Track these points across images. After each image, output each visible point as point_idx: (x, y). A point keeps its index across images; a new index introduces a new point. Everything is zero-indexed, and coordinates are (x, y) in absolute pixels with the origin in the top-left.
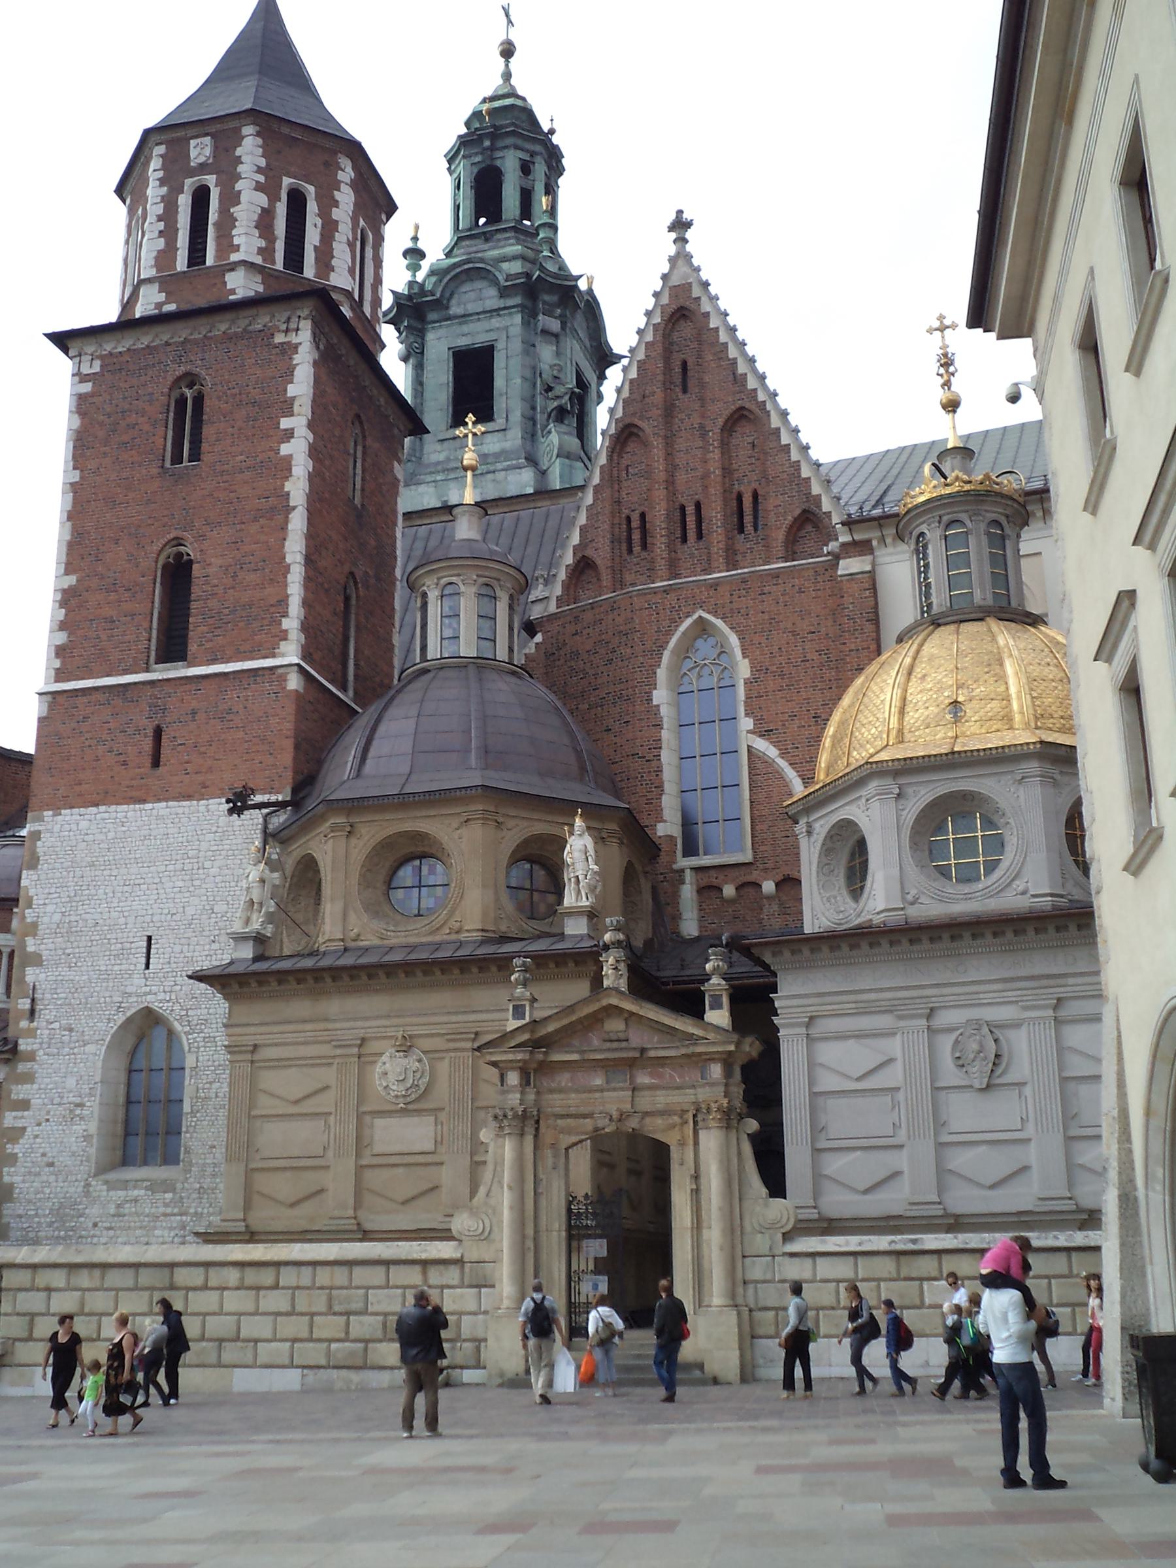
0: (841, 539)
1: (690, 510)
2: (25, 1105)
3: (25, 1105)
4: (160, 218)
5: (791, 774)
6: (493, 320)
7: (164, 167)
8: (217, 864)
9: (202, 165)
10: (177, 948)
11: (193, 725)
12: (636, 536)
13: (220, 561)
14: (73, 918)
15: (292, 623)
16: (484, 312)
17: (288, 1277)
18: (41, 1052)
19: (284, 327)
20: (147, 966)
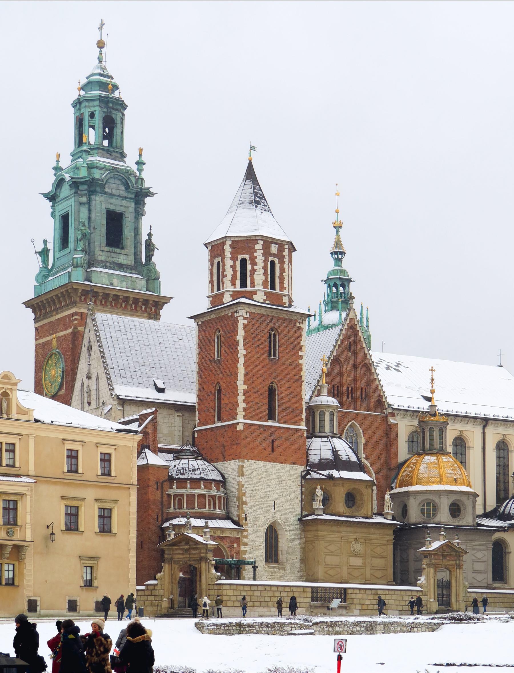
0: (390, 411)
1: (350, 389)
2: (246, 544)
3: (246, 544)
4: (263, 269)
5: (372, 471)
6: (123, 202)
7: (263, 249)
8: (290, 483)
9: (274, 254)
10: (281, 505)
11: (281, 442)
12: (336, 392)
13: (285, 392)
14: (255, 493)
15: (304, 416)
16: (119, 196)
17: (396, 593)
18: (249, 530)
19: (299, 321)
20: (274, 510)
